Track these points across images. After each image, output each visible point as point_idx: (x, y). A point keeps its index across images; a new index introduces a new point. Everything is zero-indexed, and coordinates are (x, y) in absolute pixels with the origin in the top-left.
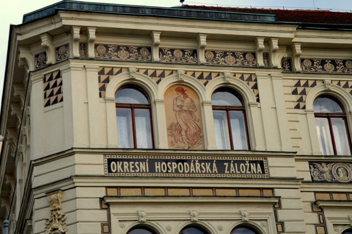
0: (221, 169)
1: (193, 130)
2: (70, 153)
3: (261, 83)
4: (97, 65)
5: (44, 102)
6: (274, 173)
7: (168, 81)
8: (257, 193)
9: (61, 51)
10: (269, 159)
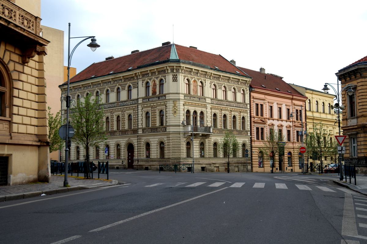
0: (199, 100)
1: (196, 91)
2: (179, 94)
3: (207, 81)
4: (183, 75)
5: (172, 80)
6: (207, 101)
7: (193, 79)
8: (204, 105)
9: (177, 70)
10: (206, 99)
